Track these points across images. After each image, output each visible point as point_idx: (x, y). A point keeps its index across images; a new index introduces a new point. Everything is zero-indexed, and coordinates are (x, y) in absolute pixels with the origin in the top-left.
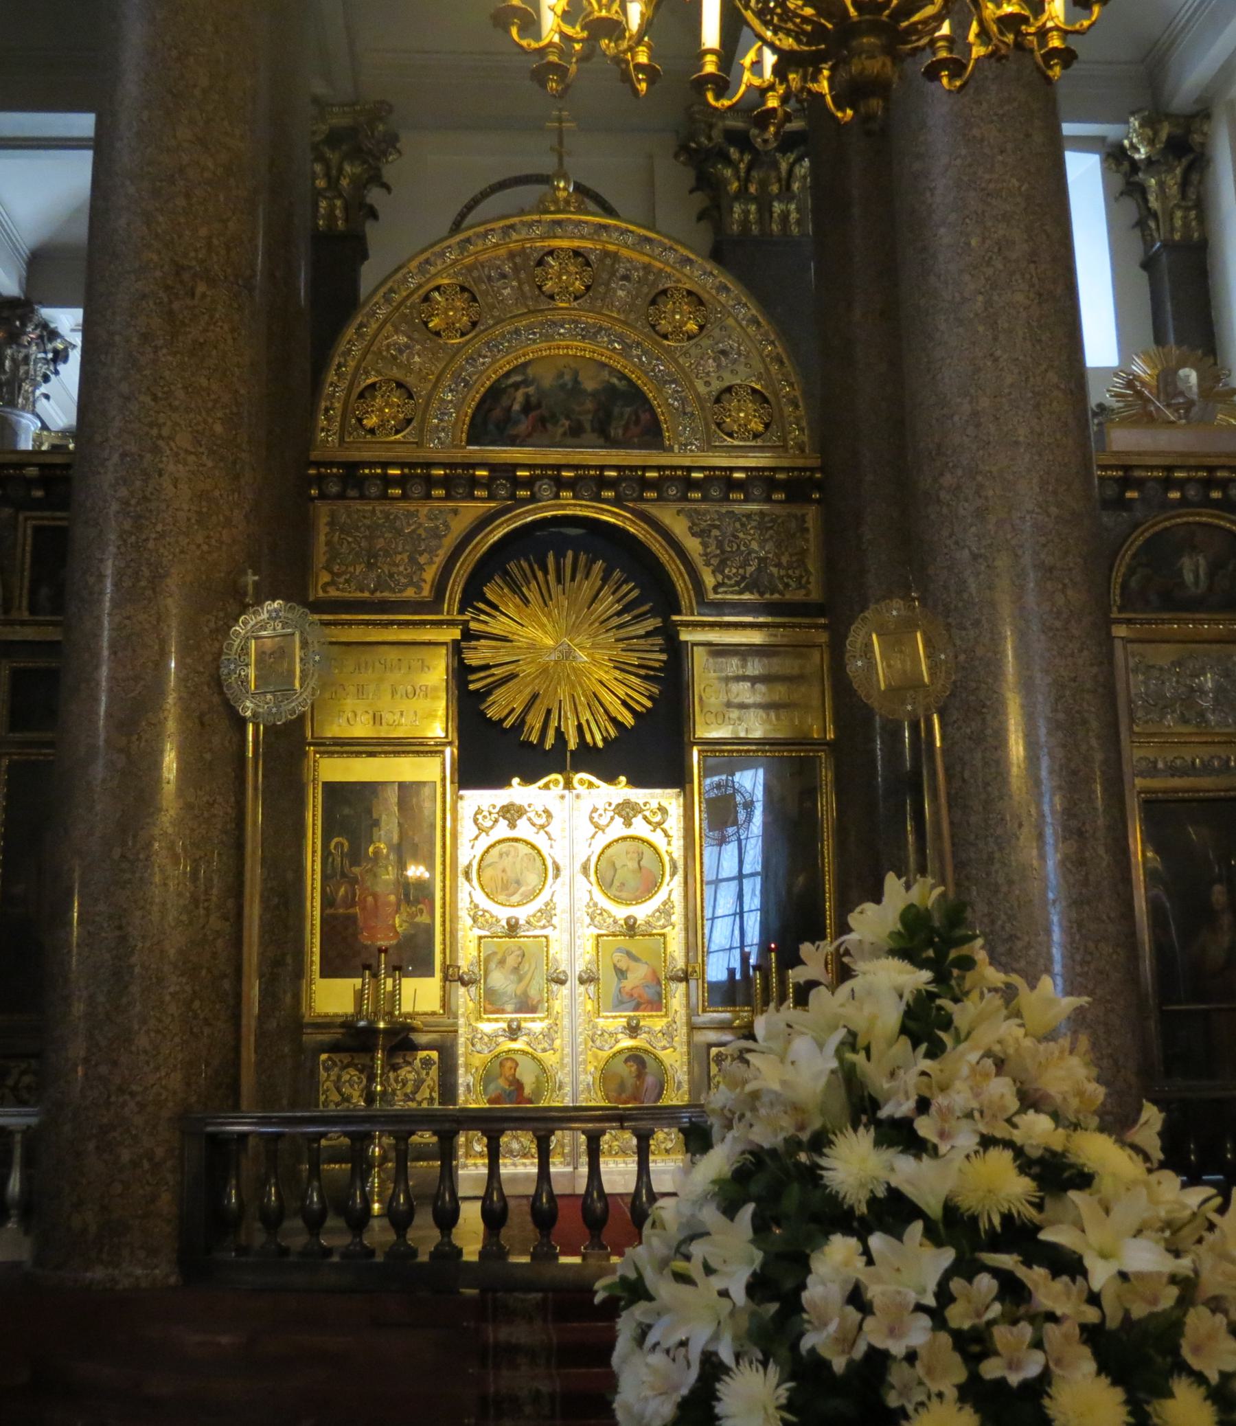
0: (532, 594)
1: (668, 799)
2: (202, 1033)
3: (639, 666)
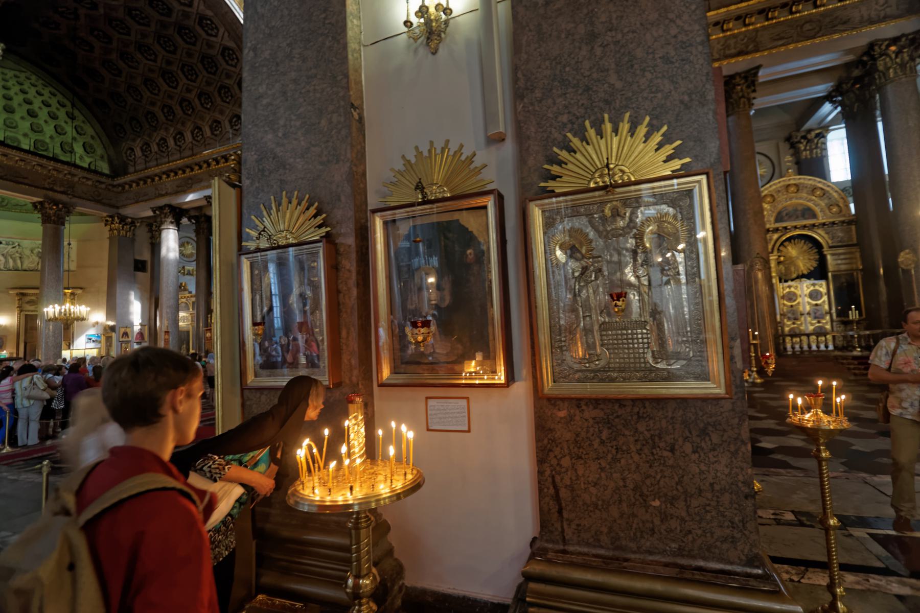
1: (823, 283)
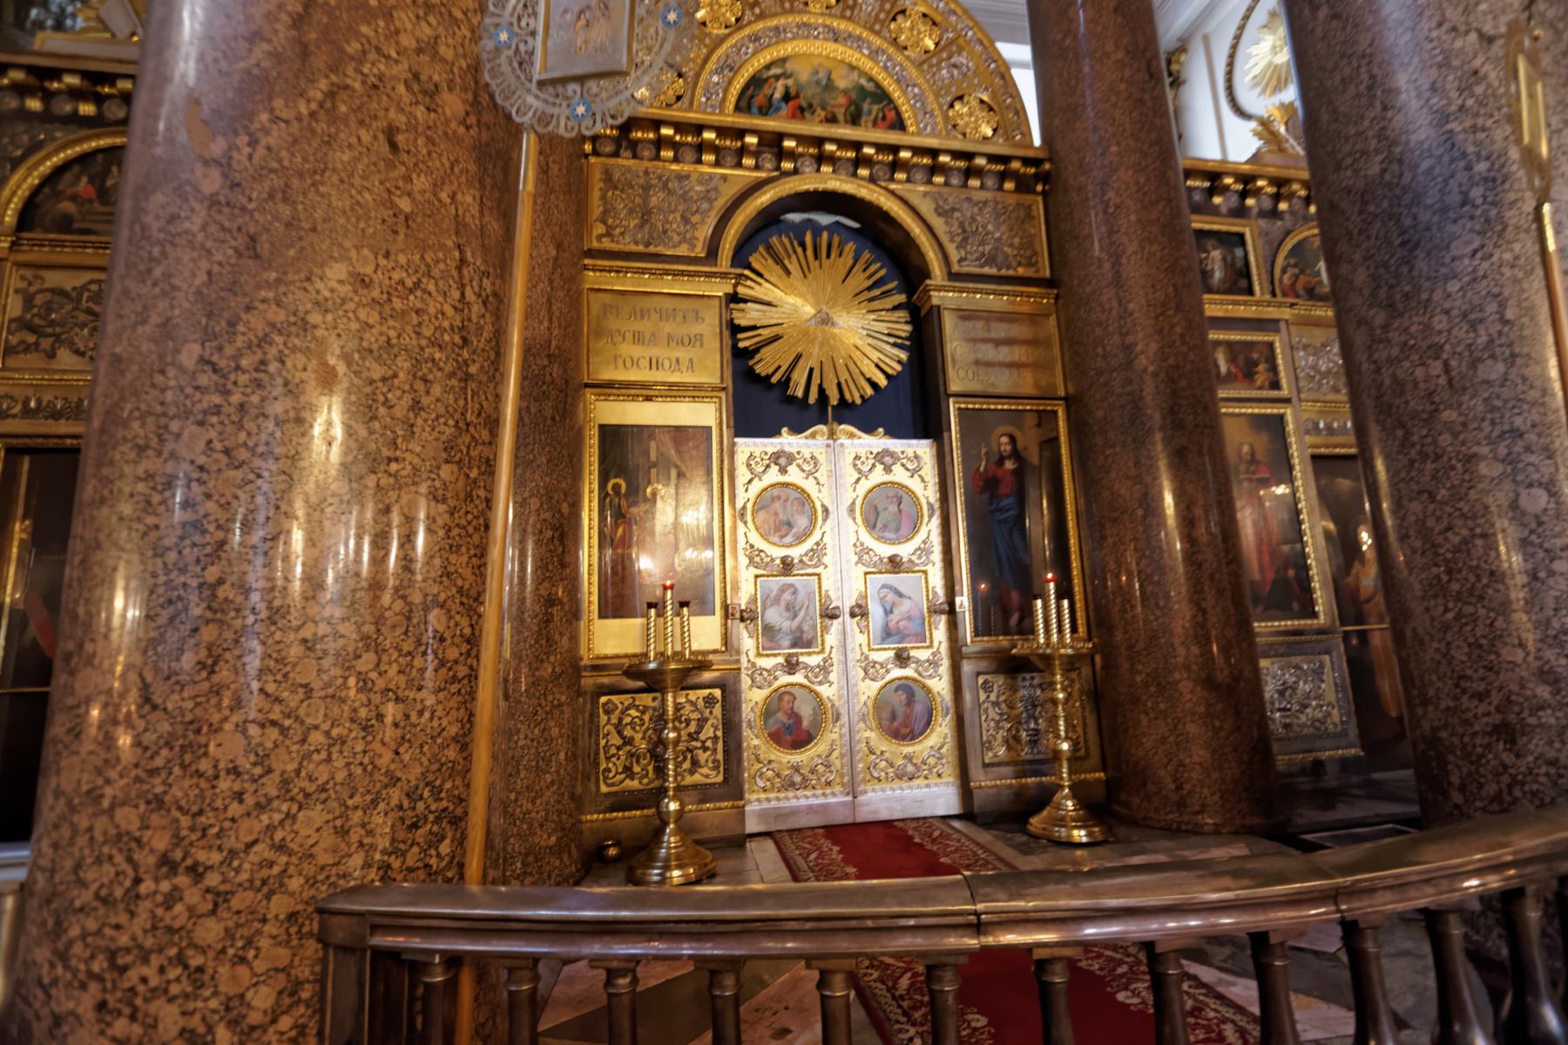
0: (793, 266)
1: (923, 449)
2: (380, 717)
3: (889, 335)
